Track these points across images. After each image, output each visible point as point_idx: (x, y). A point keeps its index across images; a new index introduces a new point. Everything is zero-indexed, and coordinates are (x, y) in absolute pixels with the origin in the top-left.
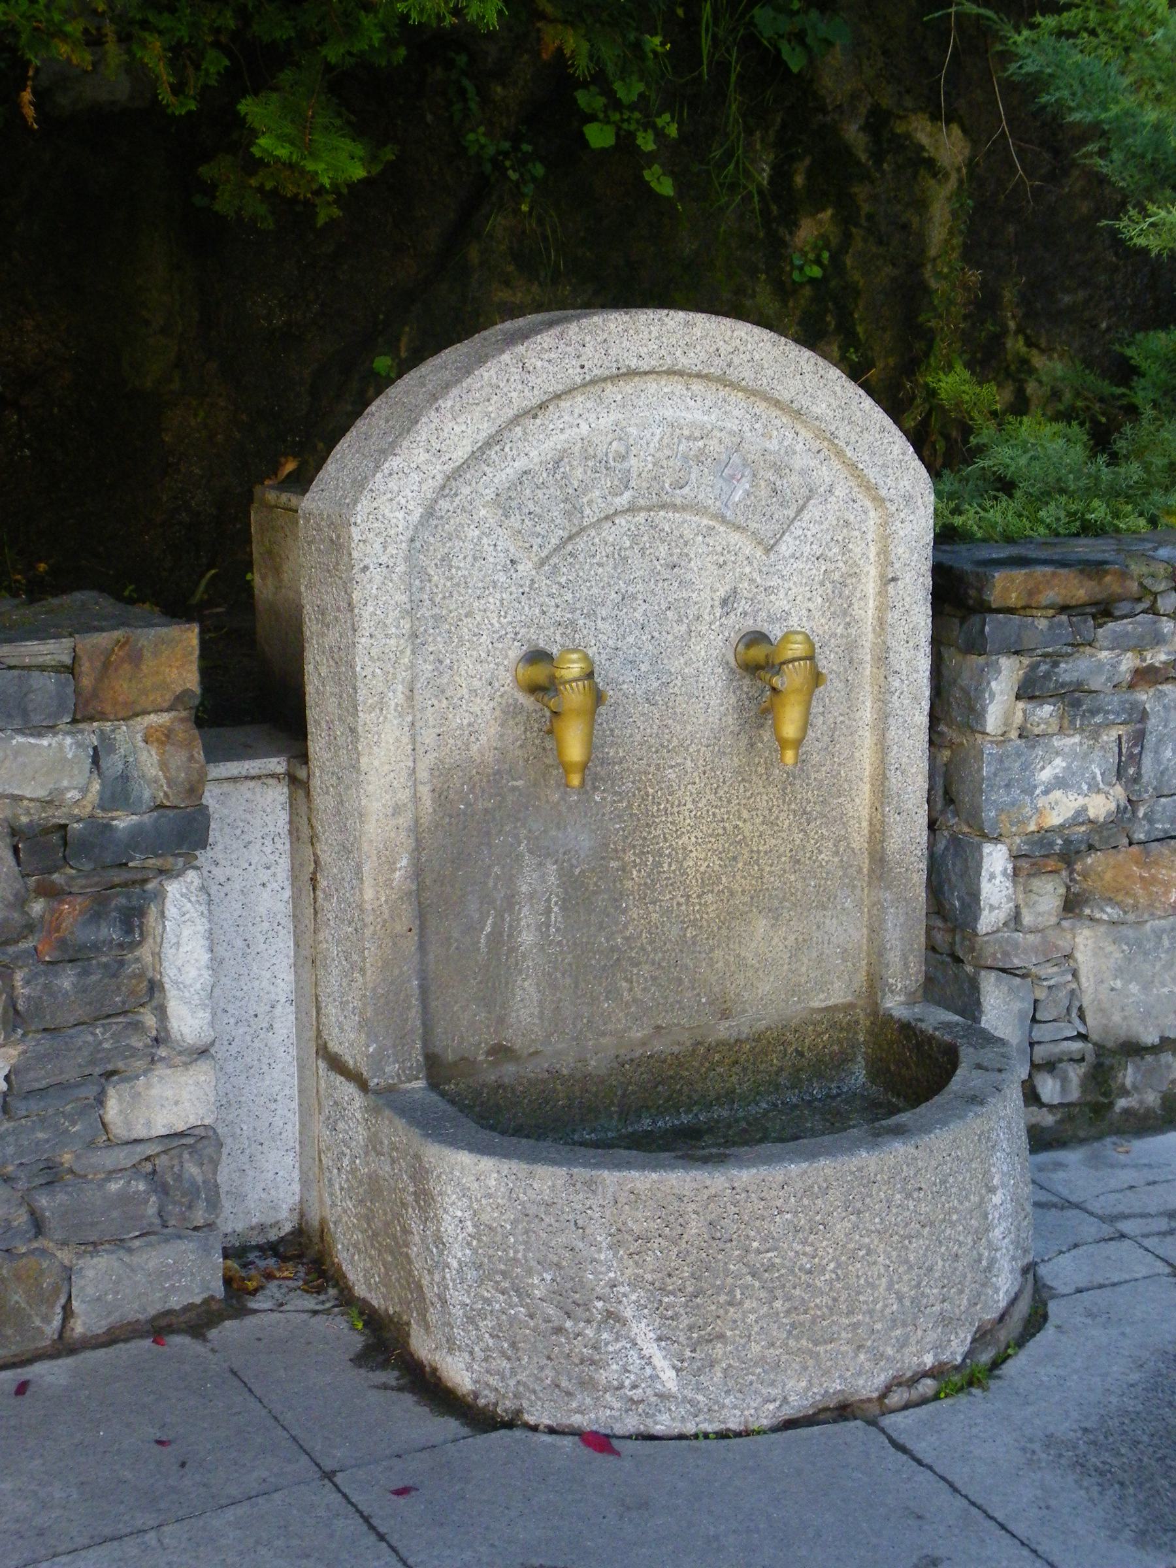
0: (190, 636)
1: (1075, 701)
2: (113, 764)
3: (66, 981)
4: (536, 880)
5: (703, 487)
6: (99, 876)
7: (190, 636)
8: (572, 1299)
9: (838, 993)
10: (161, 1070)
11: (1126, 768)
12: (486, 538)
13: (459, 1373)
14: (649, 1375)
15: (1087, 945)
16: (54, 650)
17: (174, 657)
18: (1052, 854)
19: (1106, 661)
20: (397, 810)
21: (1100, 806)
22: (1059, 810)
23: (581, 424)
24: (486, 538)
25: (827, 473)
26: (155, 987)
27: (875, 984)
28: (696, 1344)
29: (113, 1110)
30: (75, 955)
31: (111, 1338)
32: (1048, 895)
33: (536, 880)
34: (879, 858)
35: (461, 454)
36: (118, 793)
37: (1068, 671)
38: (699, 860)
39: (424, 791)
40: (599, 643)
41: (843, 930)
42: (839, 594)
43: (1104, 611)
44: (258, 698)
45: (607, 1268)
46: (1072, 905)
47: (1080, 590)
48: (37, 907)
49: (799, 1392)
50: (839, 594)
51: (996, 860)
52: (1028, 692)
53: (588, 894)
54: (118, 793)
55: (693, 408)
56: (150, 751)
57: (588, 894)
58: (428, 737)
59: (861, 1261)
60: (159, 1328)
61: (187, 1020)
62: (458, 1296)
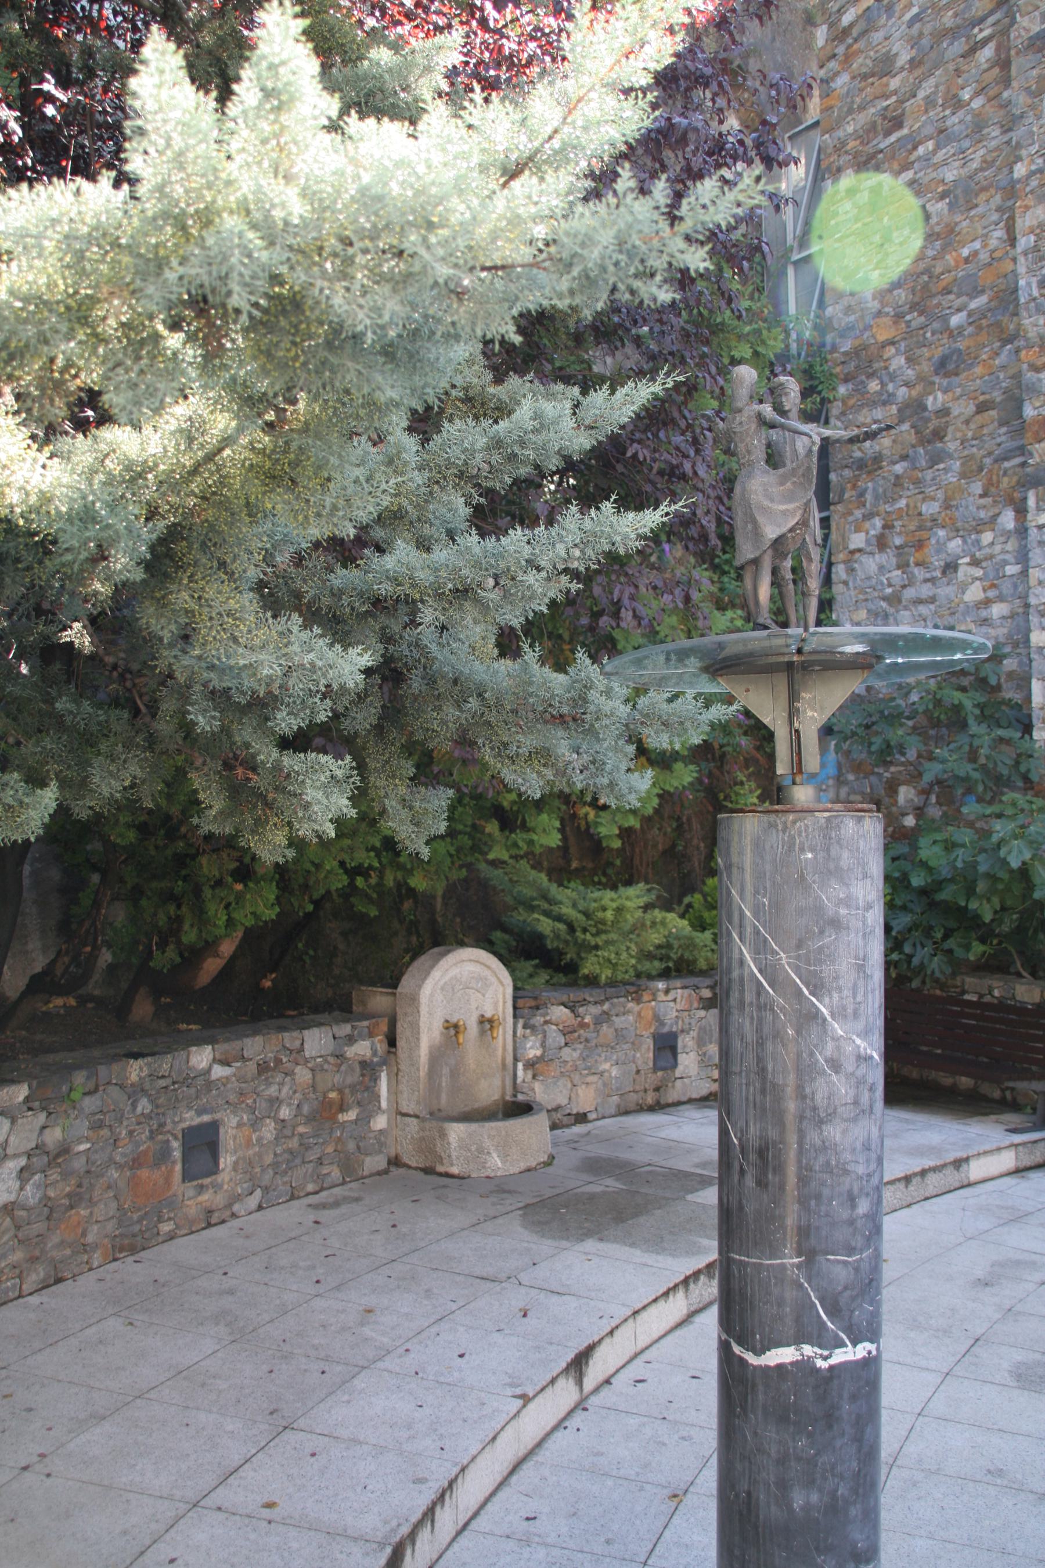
1: (533, 1028)
4: (446, 1071)
8: (481, 1150)
9: (496, 1097)
11: (543, 1045)
12: (439, 997)
13: (455, 1170)
14: (496, 1164)
15: (537, 1086)
18: (530, 1065)
19: (539, 1020)
21: (539, 1053)
23: (454, 972)
25: (493, 979)
27: (504, 1094)
28: (505, 1156)
30: (367, 1089)
31: (371, 1175)
33: (446, 1071)
34: (504, 1065)
36: (375, 1053)
37: (532, 1022)
38: (473, 1066)
41: (497, 1082)
43: (538, 1008)
45: (487, 1143)
46: (534, 1077)
47: (533, 1003)
49: (523, 1166)
51: (520, 1066)
52: (525, 1027)
53: (454, 1074)
57: (454, 1074)
59: (532, 1136)
60: (379, 1173)
62: (454, 1154)
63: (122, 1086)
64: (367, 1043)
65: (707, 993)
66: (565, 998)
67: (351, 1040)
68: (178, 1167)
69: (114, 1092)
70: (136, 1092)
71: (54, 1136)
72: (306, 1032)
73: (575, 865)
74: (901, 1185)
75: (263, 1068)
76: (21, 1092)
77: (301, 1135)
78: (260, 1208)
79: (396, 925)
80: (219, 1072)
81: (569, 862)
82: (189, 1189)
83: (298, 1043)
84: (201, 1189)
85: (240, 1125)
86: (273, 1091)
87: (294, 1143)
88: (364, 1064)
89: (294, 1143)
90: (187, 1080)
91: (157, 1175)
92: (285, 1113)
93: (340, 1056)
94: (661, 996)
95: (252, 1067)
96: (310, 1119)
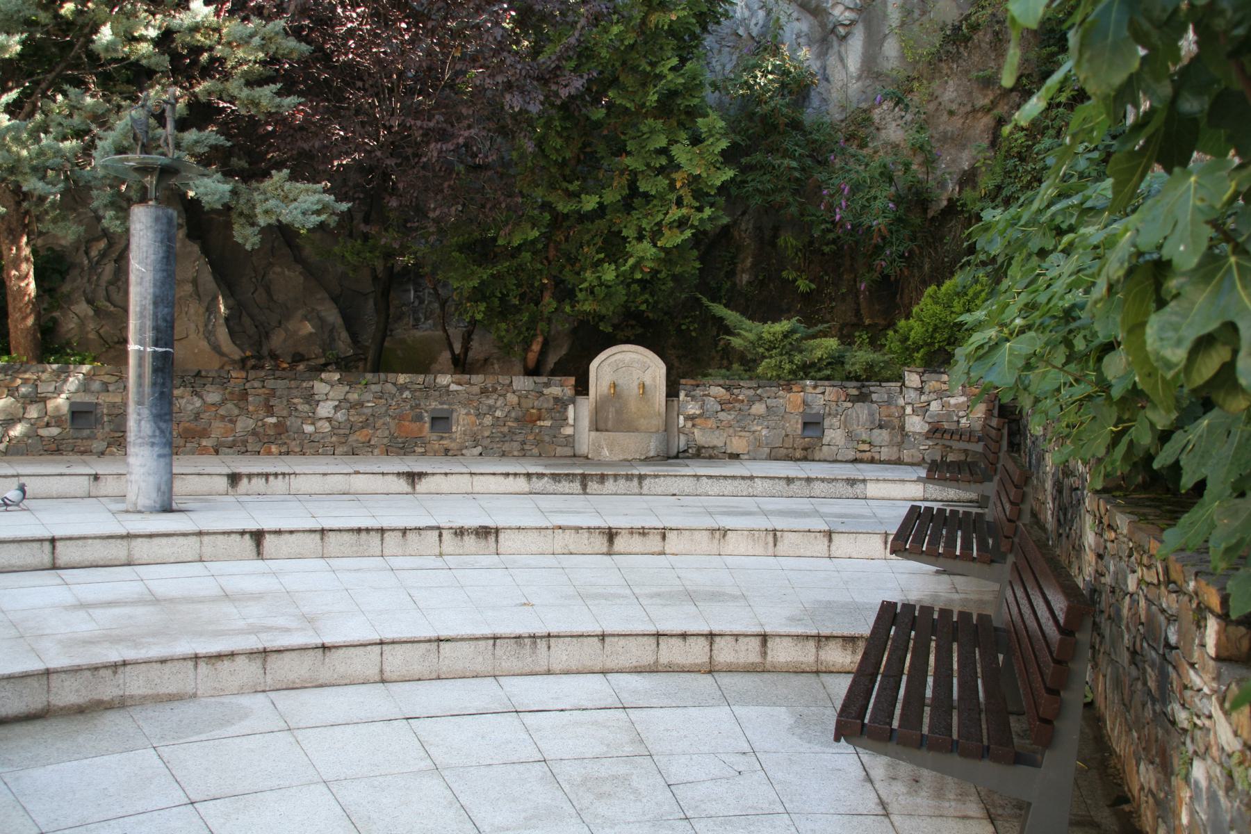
1: (693, 398)
4: (612, 410)
5: (635, 365)
6: (561, 403)
11: (702, 407)
17: (572, 380)
19: (698, 392)
22: (691, 412)
24: (606, 368)
28: (611, 451)
32: (689, 424)
33: (612, 410)
38: (634, 410)
40: (620, 382)
42: (654, 379)
44: (582, 388)
45: (603, 443)
49: (621, 457)
50: (654, 379)
51: (681, 418)
53: (619, 412)
55: (634, 356)
56: (569, 392)
57: (619, 412)
61: (571, 421)
63: (394, 384)
65: (855, 392)
66: (721, 382)
67: (547, 385)
68: (427, 425)
69: (389, 386)
70: (402, 388)
71: (354, 397)
73: (867, 322)
74: (783, 483)
75: (484, 391)
76: (337, 376)
79: (713, 353)
80: (453, 387)
81: (861, 319)
82: (434, 436)
83: (508, 382)
84: (442, 438)
85: (468, 414)
86: (491, 402)
87: (506, 429)
88: (556, 399)
89: (506, 429)
90: (436, 388)
91: (415, 426)
92: (498, 414)
93: (542, 394)
94: (810, 390)
95: (476, 389)
96: (517, 420)
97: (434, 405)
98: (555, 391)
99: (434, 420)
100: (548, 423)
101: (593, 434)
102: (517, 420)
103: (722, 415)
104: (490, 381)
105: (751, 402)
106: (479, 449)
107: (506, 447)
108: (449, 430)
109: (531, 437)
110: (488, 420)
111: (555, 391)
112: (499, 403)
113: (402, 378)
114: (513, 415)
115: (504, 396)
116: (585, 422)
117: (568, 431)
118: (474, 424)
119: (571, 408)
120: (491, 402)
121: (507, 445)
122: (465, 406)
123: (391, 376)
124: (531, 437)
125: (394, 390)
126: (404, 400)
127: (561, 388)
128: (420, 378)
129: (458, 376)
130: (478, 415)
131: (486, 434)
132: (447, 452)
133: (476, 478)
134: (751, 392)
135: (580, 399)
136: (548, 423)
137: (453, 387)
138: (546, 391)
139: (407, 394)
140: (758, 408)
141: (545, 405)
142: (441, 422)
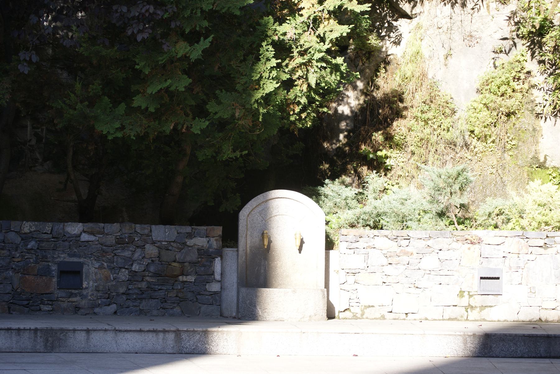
0: (221, 228)
2: (210, 242)
3: (202, 269)
6: (208, 256)
7: (221, 228)
10: (213, 283)
16: (205, 228)
17: (219, 230)
20: (243, 250)
26: (214, 272)
29: (207, 287)
30: (204, 266)
35: (254, 206)
39: (248, 249)
48: (200, 259)
54: (210, 246)
56: (215, 243)
58: (249, 242)
61: (218, 277)
64: (205, 240)
67: (190, 236)
68: (55, 280)
70: (26, 238)
72: (153, 227)
75: (120, 241)
77: (148, 282)
78: (115, 313)
84: (71, 295)
85: (101, 267)
86: (127, 254)
87: (144, 285)
88: (201, 252)
89: (144, 285)
90: (65, 237)
92: (135, 267)
95: (111, 240)
96: (156, 275)
97: (64, 257)
98: (200, 242)
99: (63, 273)
100: (191, 278)
101: (243, 290)
102: (156, 275)
103: (389, 270)
104: (127, 229)
105: (421, 254)
106: (114, 307)
107: (144, 305)
108: (79, 286)
109: (172, 294)
110: (124, 275)
111: (200, 242)
112: (136, 255)
113: (27, 227)
114: (152, 269)
115: (143, 247)
116: (232, 279)
117: (215, 287)
118: (107, 279)
119: (218, 261)
120: (127, 254)
121: (144, 303)
122: (98, 259)
123: (14, 225)
124: (172, 294)
125: (18, 240)
126: (29, 251)
127: (205, 239)
128: (48, 227)
129: (90, 225)
130: (112, 269)
131: (122, 290)
132: (77, 309)
133: (121, 335)
134: (423, 244)
135: (229, 252)
136: (191, 278)
137: (85, 237)
138: (190, 242)
139: (32, 244)
140: (430, 262)
141: (188, 259)
142: (72, 275)
